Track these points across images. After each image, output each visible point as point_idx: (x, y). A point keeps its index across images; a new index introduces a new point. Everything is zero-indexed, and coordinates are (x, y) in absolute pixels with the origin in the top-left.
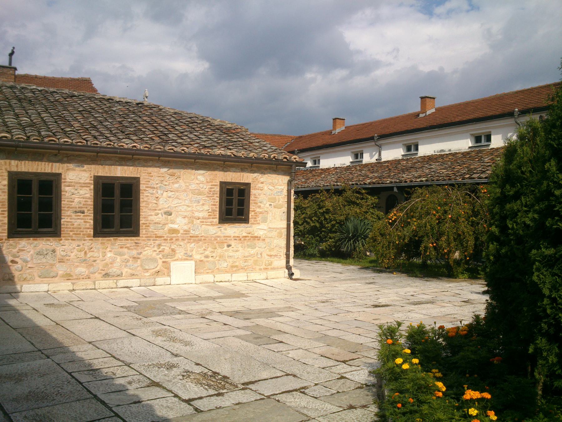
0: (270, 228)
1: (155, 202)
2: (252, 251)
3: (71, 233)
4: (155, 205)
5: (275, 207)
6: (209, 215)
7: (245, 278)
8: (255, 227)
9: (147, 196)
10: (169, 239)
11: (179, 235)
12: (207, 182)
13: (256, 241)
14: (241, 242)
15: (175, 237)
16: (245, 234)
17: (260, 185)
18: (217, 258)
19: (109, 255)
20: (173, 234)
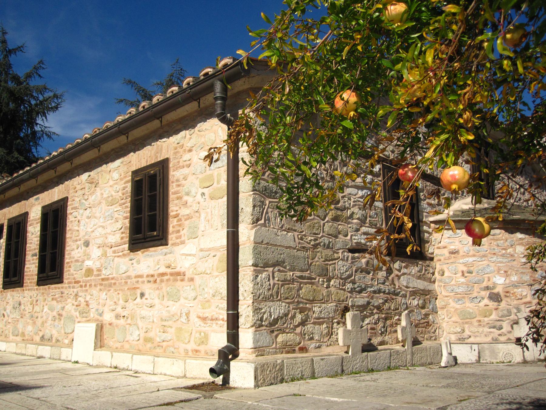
0: (202, 250)
1: (76, 228)
2: (174, 308)
3: (29, 281)
4: (77, 233)
5: (212, 198)
6: (122, 238)
7: (149, 369)
8: (180, 250)
9: (72, 221)
10: (84, 284)
11: (92, 278)
12: (121, 179)
13: (179, 283)
14: (155, 286)
15: (88, 281)
16: (163, 270)
17: (187, 157)
18: (129, 321)
19: (46, 309)
20: (88, 276)
